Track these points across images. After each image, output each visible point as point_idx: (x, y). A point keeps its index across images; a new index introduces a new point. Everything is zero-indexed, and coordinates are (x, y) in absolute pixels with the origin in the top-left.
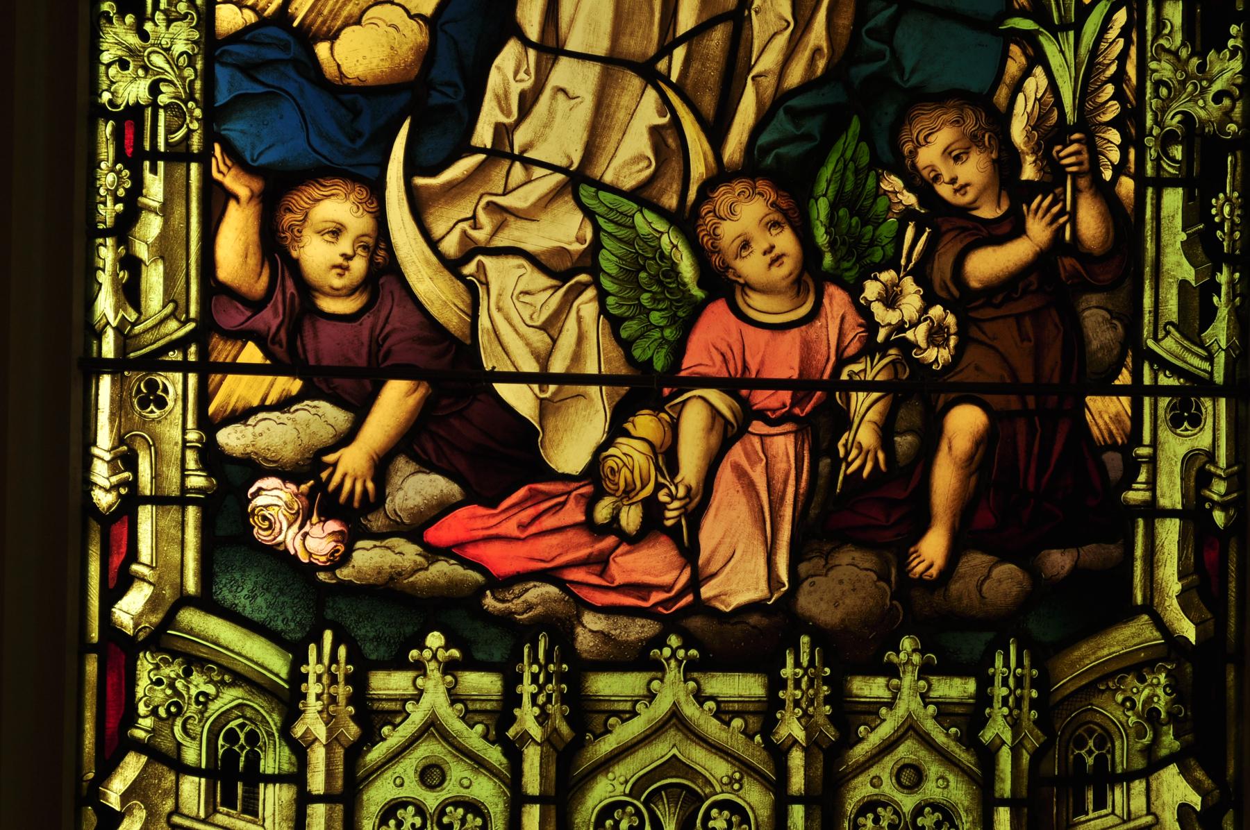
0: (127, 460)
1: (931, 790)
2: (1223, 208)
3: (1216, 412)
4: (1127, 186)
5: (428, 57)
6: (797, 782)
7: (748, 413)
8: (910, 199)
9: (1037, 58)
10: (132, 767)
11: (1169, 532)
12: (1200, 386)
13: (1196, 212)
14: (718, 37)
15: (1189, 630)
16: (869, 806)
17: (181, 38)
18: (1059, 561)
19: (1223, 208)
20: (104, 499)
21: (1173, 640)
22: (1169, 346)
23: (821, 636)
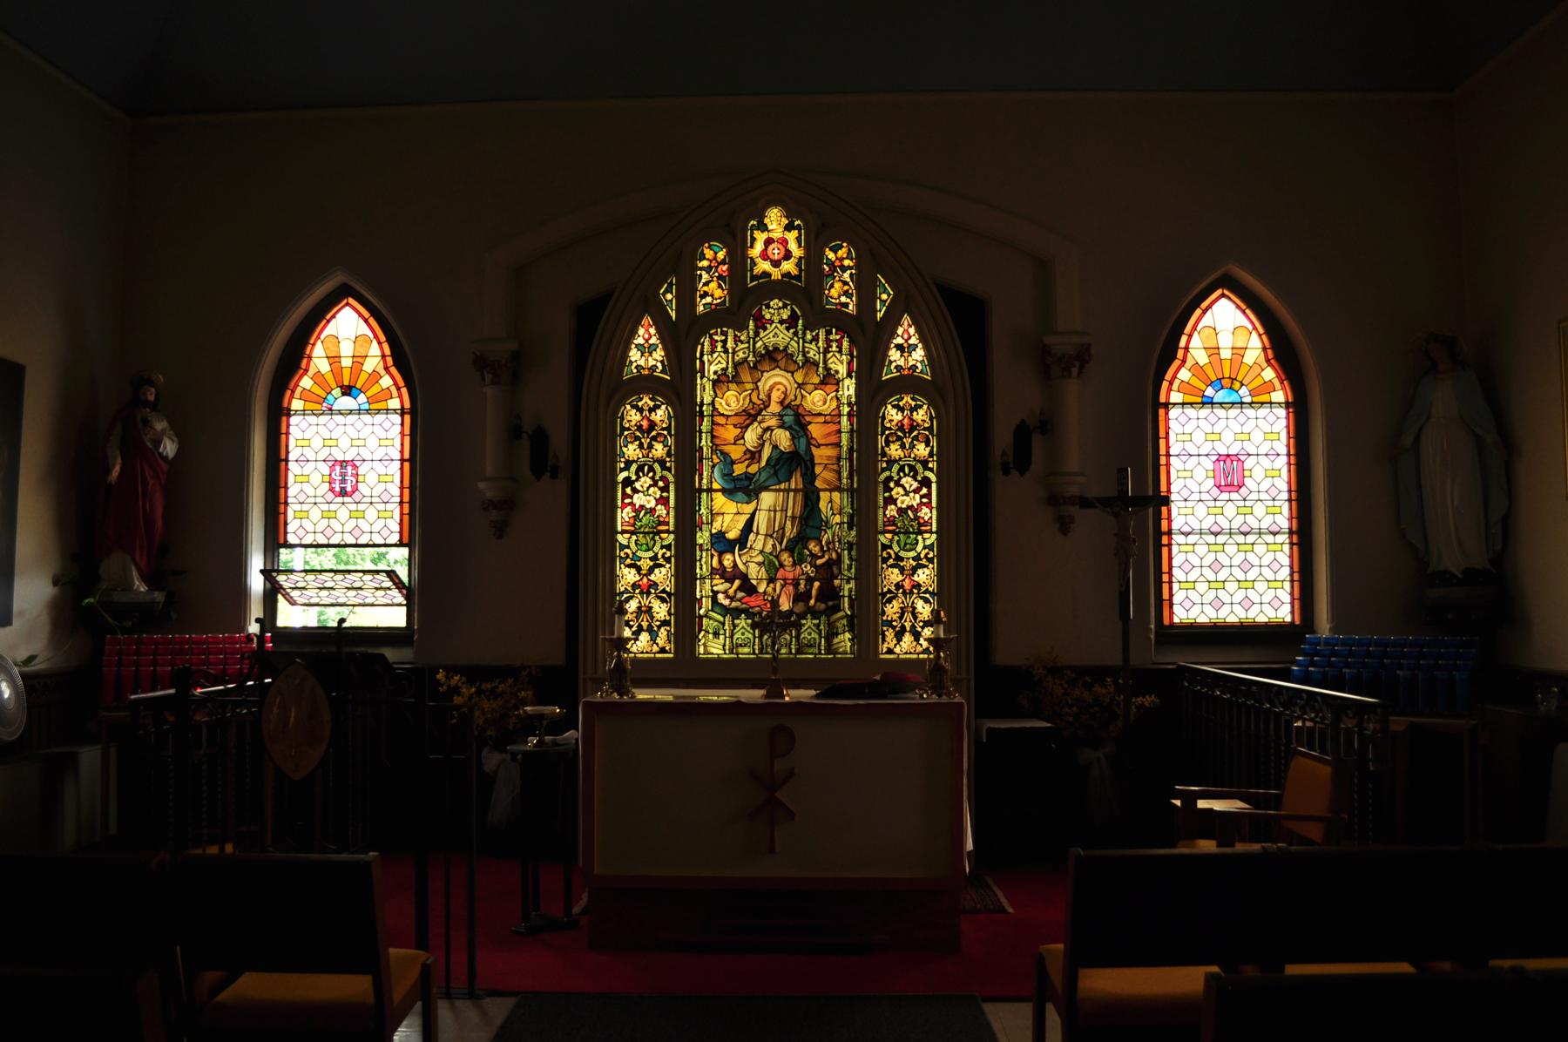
0: (701, 592)
1: (813, 636)
2: (853, 553)
3: (853, 582)
4: (839, 550)
5: (741, 535)
6: (794, 635)
7: (786, 583)
8: (808, 553)
9: (826, 532)
10: (703, 633)
11: (846, 599)
12: (850, 578)
13: (849, 554)
14: (781, 531)
15: (849, 613)
16: (804, 638)
17: (708, 534)
18: (830, 603)
19: (853, 553)
20: (698, 597)
21: (847, 615)
22: (846, 573)
23: (797, 614)
